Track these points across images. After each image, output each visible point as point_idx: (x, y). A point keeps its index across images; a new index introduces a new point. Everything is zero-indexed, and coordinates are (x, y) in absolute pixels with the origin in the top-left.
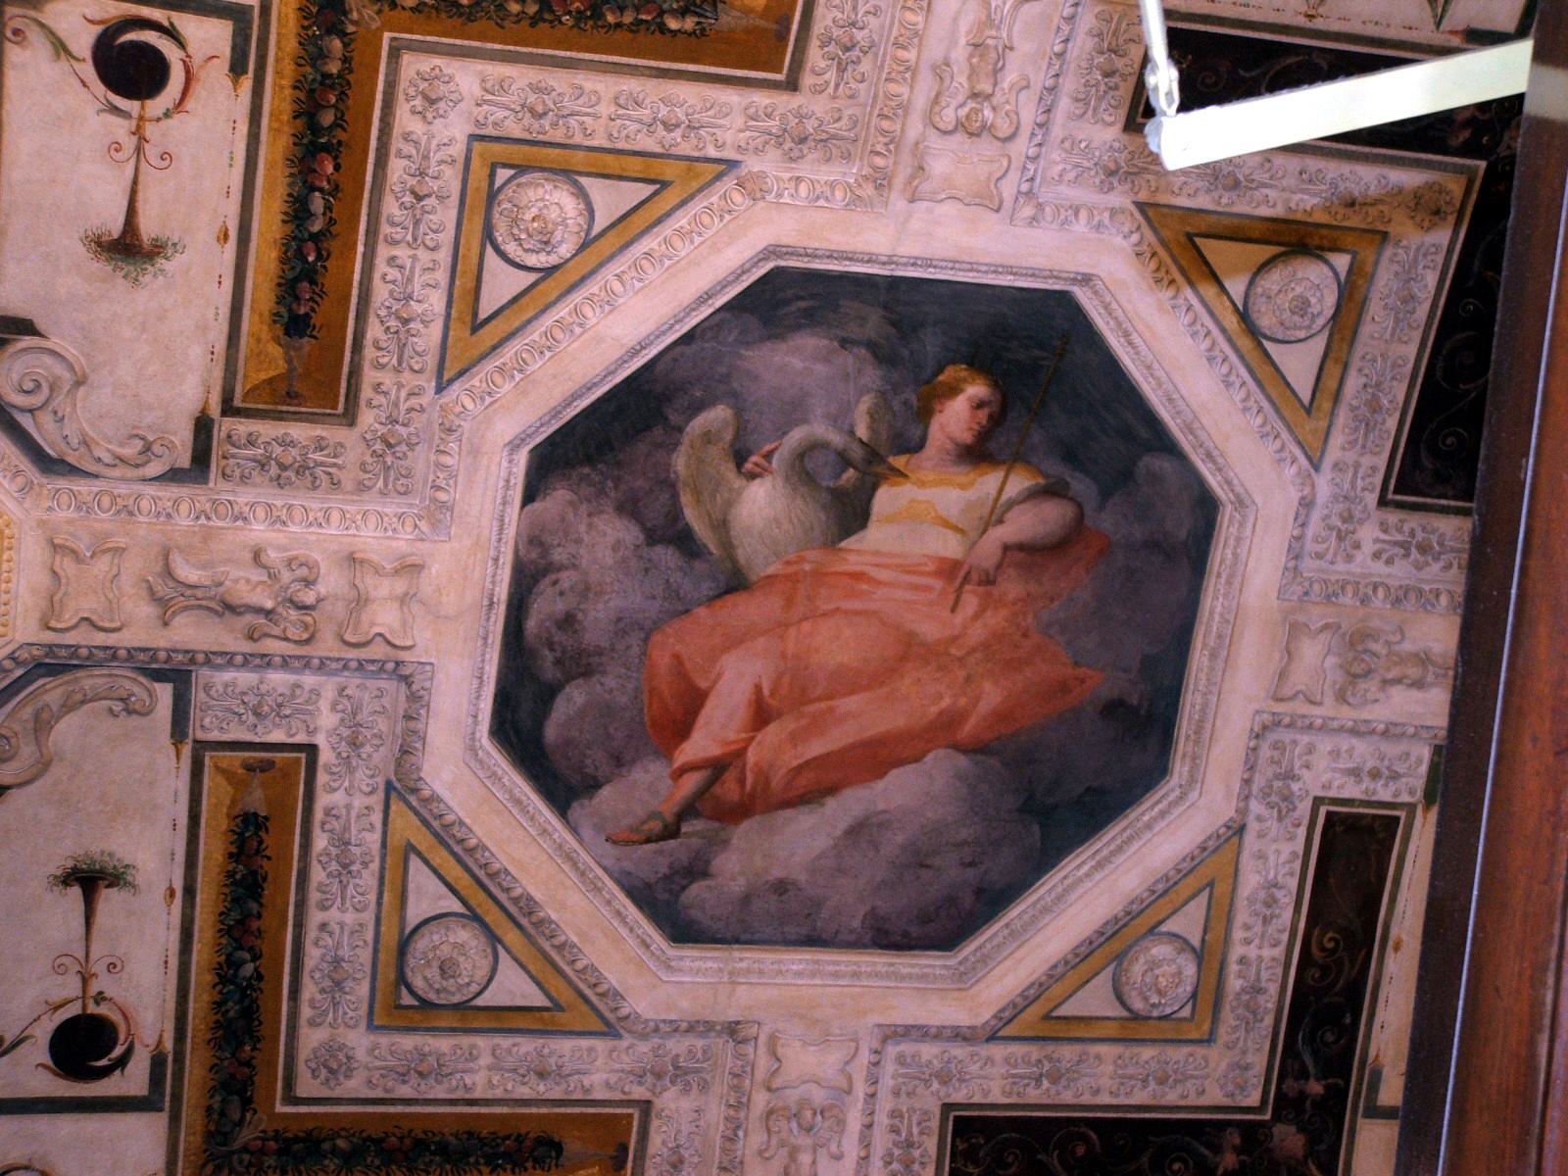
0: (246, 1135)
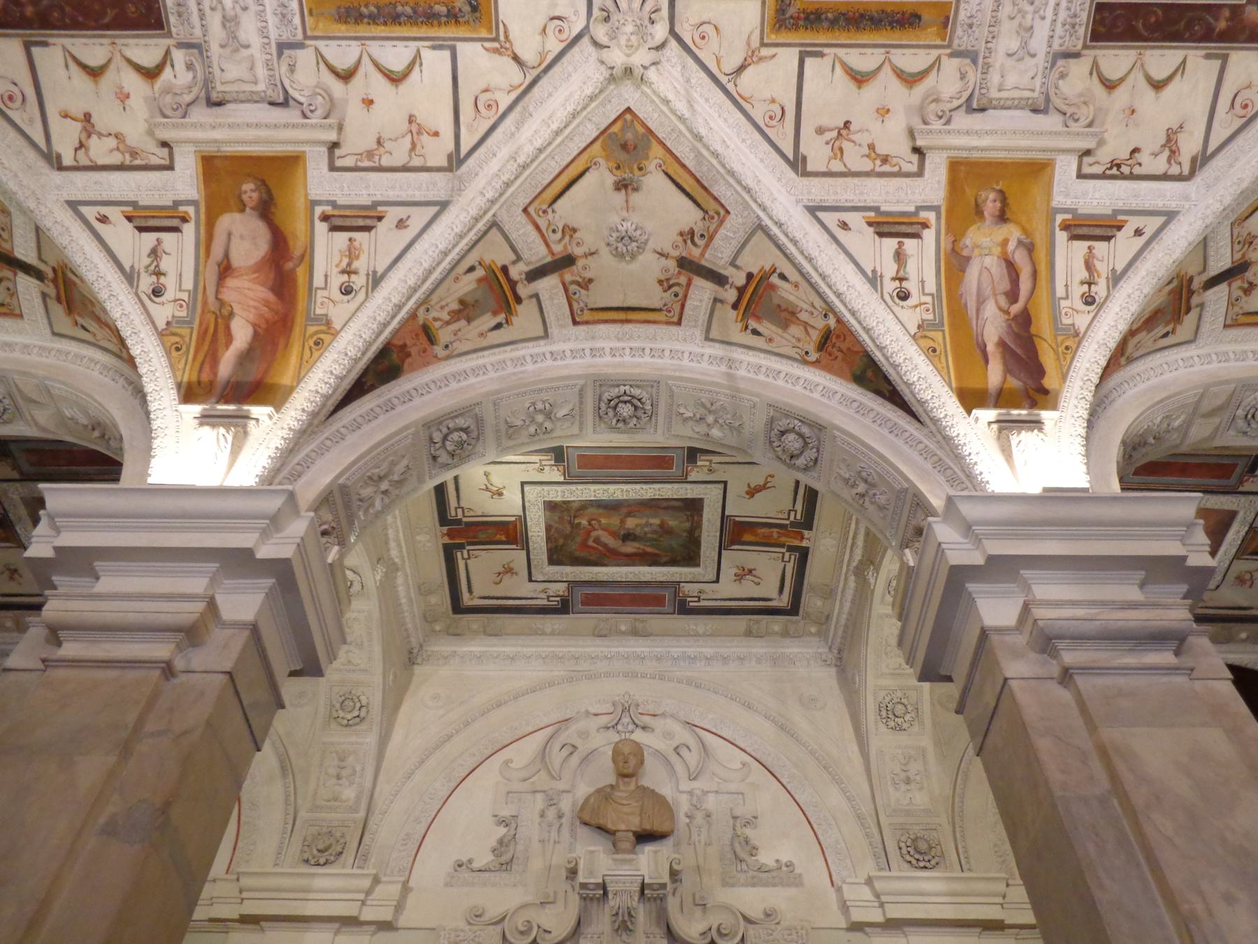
0: (792, 11)
